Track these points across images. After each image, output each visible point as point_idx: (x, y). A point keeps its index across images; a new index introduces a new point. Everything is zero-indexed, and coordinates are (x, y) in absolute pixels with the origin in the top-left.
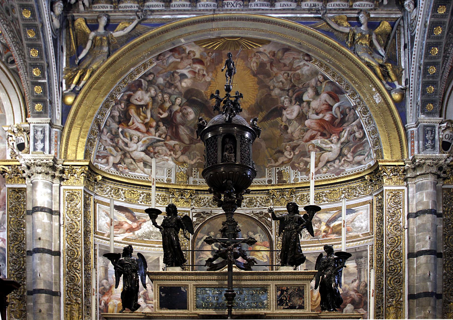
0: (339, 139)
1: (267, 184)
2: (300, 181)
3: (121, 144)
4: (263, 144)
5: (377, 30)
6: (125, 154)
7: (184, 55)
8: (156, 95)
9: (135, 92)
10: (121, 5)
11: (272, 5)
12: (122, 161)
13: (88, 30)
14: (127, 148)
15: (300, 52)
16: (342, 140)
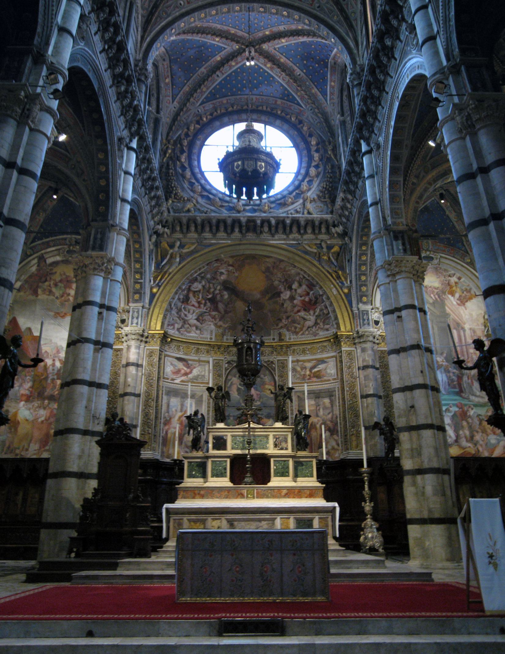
0: (314, 313)
1: (272, 341)
2: (292, 340)
3: (183, 315)
4: (269, 314)
5: (333, 251)
6: (185, 322)
7: (222, 262)
8: (206, 285)
9: (193, 283)
10: (189, 235)
11: (273, 236)
12: (182, 326)
13: (168, 248)
14: (186, 318)
15: (289, 263)
16: (317, 314)
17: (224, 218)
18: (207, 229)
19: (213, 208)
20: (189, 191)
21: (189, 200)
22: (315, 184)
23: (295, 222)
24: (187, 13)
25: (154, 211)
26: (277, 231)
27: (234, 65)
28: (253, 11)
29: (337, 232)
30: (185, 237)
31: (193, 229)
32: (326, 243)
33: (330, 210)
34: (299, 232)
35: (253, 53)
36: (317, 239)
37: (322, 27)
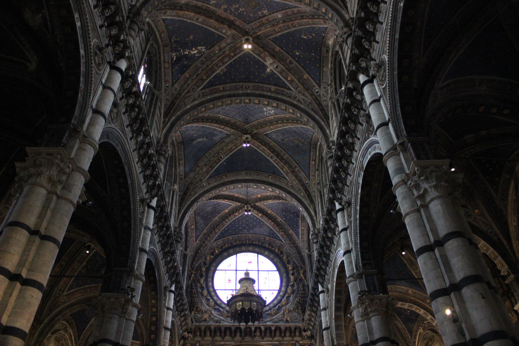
11: (263, 338)
17: (229, 326)
18: (218, 334)
19: (222, 318)
20: (206, 306)
21: (206, 312)
22: (291, 298)
23: (278, 328)
24: (207, 191)
25: (183, 324)
26: (265, 335)
27: (237, 215)
28: (250, 187)
29: (306, 335)
30: (203, 340)
31: (208, 334)
32: (299, 343)
33: (302, 318)
34: (280, 335)
35: (250, 208)
36: (293, 340)
37: (294, 200)
